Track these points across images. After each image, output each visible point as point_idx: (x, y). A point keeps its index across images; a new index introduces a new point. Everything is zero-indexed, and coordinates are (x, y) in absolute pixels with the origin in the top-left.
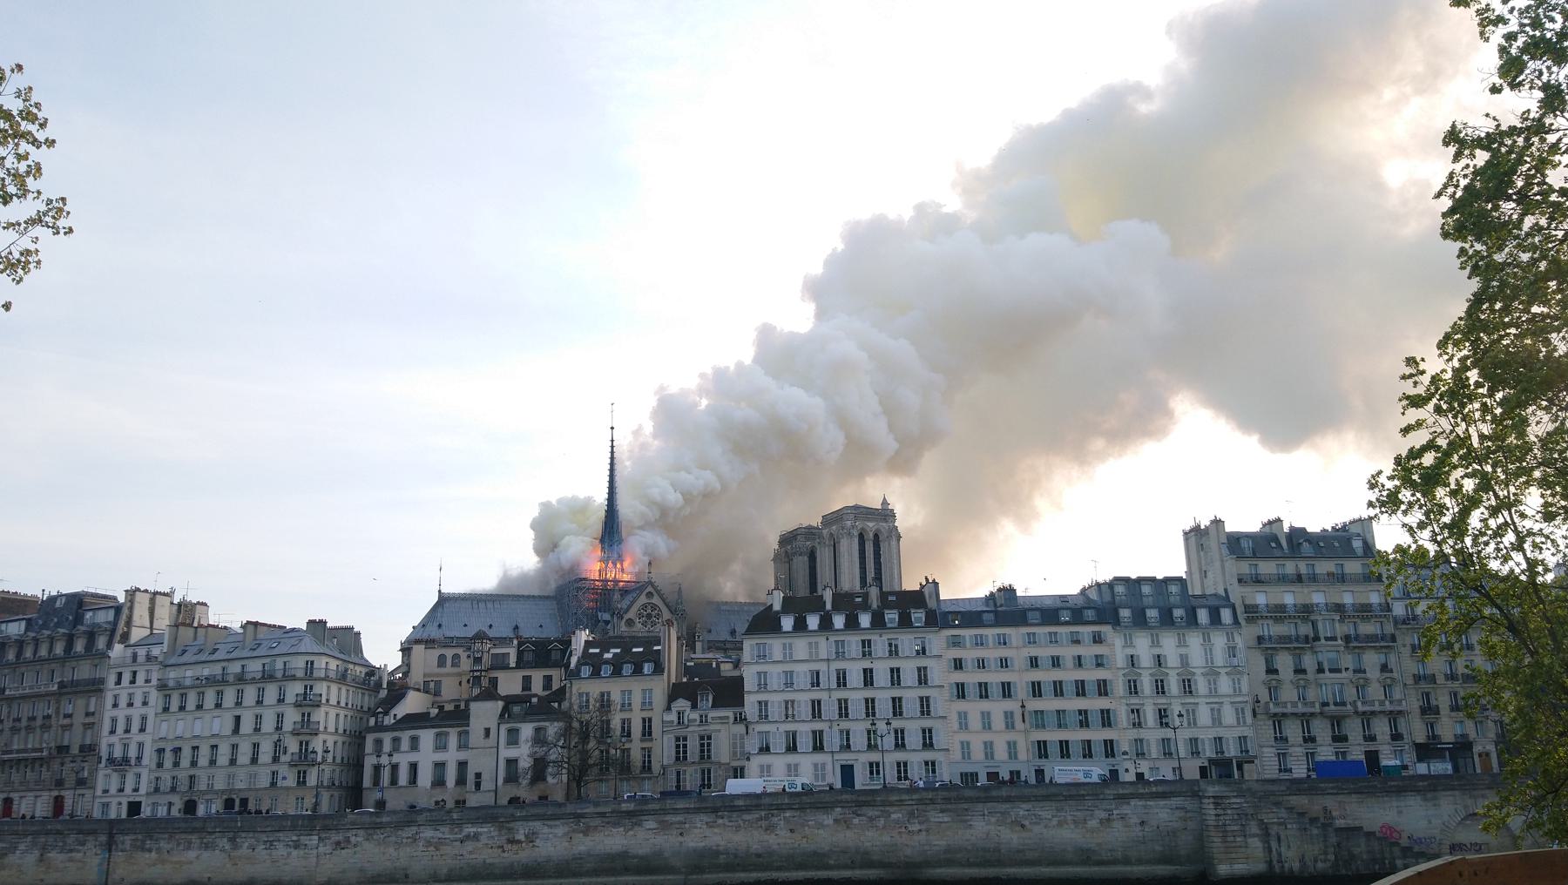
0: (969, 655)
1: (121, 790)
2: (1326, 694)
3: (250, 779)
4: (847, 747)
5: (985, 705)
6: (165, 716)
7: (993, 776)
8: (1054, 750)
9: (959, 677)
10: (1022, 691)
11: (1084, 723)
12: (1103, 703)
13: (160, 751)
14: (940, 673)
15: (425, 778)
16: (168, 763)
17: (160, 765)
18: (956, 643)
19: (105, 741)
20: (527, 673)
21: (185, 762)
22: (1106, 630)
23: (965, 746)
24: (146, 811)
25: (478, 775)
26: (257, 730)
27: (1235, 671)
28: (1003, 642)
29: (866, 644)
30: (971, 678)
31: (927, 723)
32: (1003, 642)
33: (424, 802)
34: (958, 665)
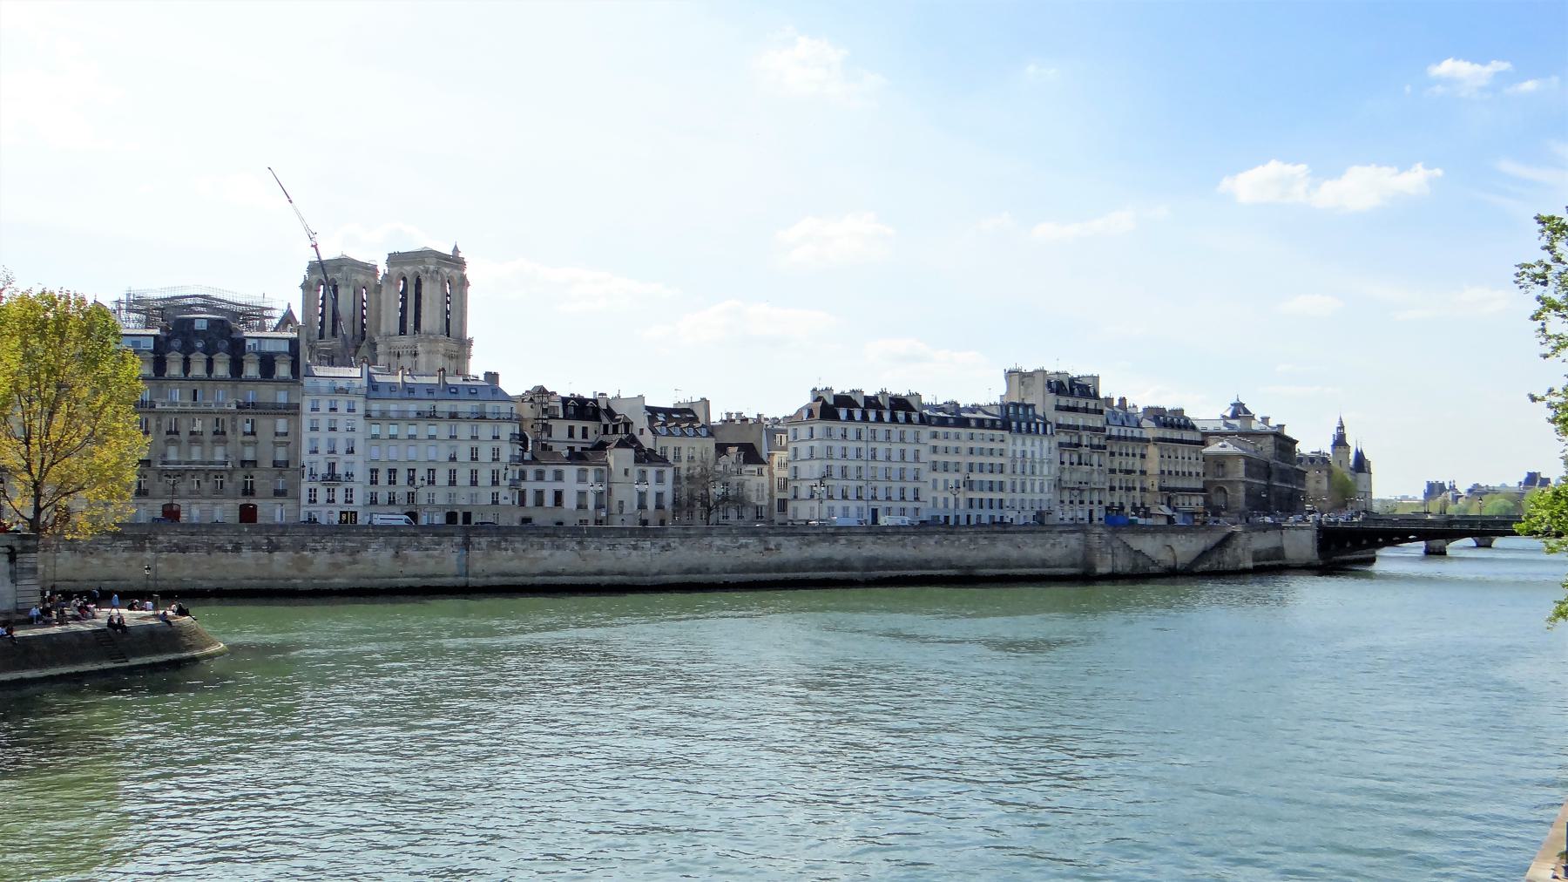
0: (941, 443)
1: (331, 501)
2: (1076, 477)
3: (478, 498)
4: (874, 498)
5: (946, 476)
6: (375, 442)
7: (947, 518)
8: (975, 504)
9: (935, 457)
10: (964, 469)
11: (991, 489)
12: (1000, 477)
13: (374, 471)
14: (926, 455)
15: (570, 502)
16: (383, 478)
17: (374, 482)
18: (935, 436)
19: (306, 458)
20: (571, 423)
21: (402, 478)
22: (1006, 433)
23: (935, 499)
24: (362, 519)
25: (621, 502)
26: (474, 459)
27: (1050, 462)
28: (958, 437)
29: (902, 433)
30: (941, 458)
31: (917, 485)
32: (958, 437)
33: (571, 521)
34: (935, 449)
